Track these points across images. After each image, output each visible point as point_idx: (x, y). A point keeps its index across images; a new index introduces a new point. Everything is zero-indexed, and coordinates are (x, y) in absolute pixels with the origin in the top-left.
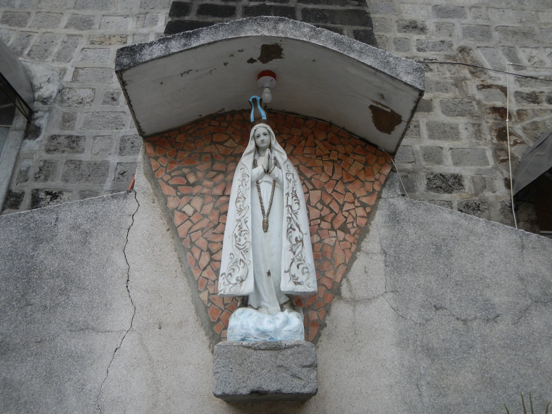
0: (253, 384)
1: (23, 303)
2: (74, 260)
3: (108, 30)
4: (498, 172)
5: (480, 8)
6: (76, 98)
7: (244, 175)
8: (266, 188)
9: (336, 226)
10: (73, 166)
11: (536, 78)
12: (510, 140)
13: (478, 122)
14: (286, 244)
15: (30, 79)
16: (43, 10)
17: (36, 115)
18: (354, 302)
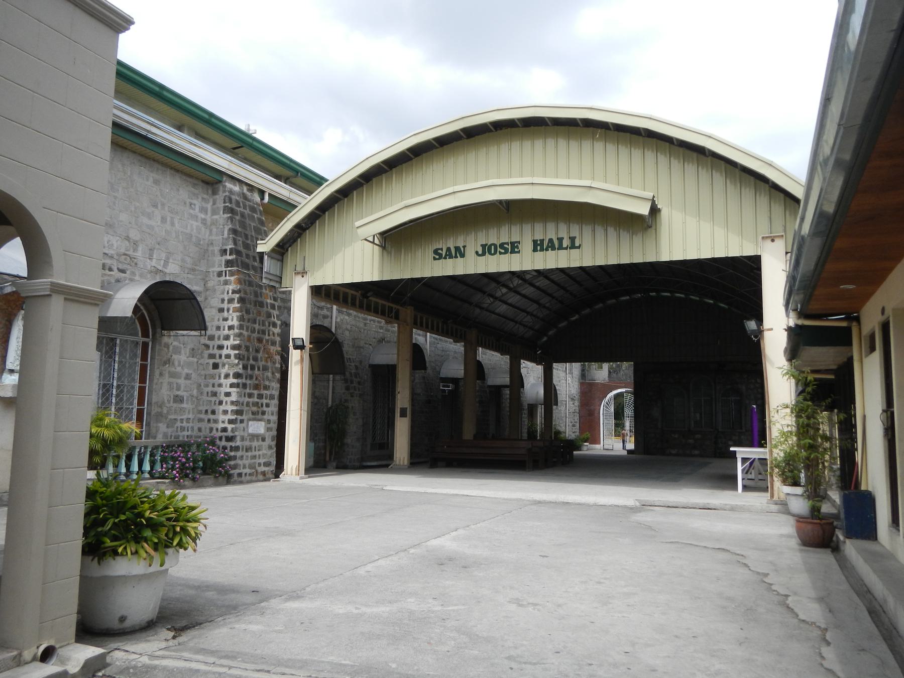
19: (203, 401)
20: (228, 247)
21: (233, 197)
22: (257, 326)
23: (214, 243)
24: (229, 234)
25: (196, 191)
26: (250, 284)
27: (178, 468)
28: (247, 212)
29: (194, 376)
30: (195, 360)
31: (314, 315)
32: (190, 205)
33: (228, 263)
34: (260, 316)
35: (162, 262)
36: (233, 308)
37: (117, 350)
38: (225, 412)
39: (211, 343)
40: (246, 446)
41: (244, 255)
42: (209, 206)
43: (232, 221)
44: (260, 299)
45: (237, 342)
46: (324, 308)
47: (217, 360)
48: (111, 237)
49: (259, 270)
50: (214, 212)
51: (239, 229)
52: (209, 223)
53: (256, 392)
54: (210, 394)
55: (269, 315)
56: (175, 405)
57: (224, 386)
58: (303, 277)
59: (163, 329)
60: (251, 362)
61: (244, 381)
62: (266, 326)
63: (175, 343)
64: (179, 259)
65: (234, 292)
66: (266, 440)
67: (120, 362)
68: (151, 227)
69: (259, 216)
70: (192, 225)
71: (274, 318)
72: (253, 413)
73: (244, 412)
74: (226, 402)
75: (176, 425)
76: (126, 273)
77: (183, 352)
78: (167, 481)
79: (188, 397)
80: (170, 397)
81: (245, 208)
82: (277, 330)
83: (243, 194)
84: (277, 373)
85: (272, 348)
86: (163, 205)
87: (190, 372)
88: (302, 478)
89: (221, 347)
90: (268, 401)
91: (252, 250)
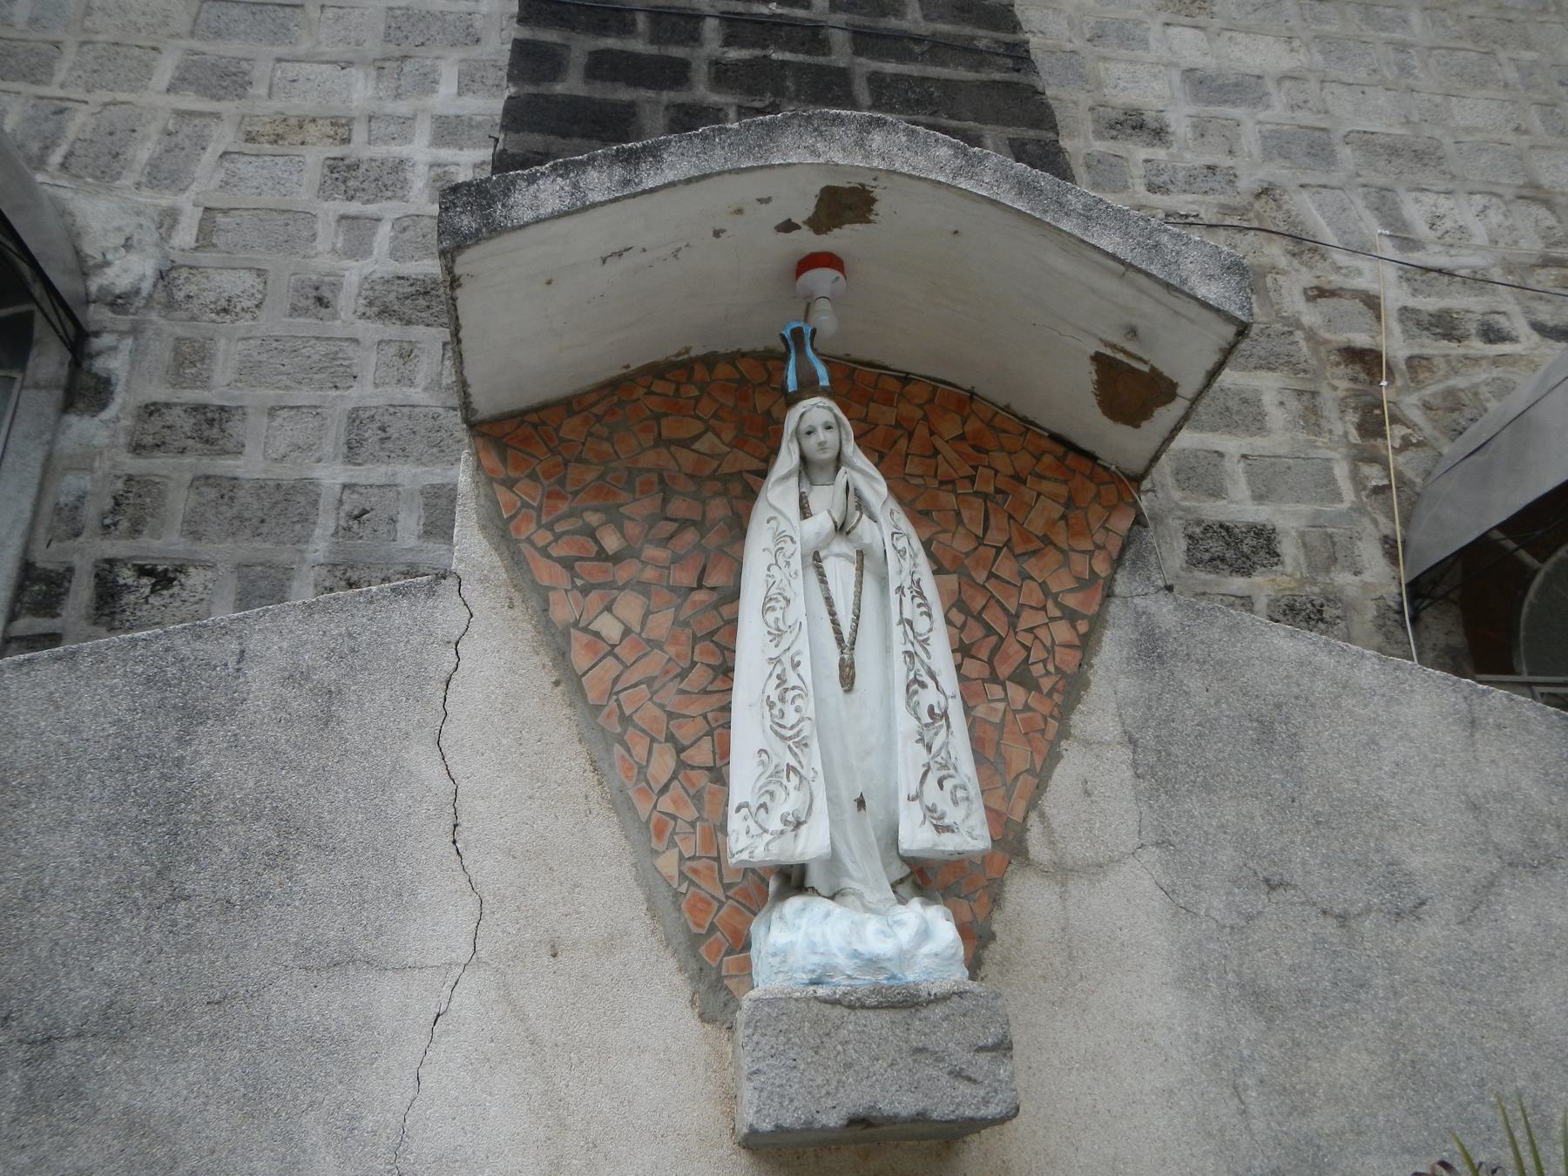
0: (854, 1098)
1: (163, 893)
2: (298, 769)
3: (296, 101)
4: (1366, 521)
5: (1306, 80)
6: (212, 297)
7: (780, 537)
8: (840, 572)
9: (1004, 671)
10: (212, 494)
11: (1451, 274)
12: (1395, 434)
13: (1310, 387)
14: (905, 724)
15: (73, 236)
16: (101, 38)
17: (97, 343)
18: (1061, 872)
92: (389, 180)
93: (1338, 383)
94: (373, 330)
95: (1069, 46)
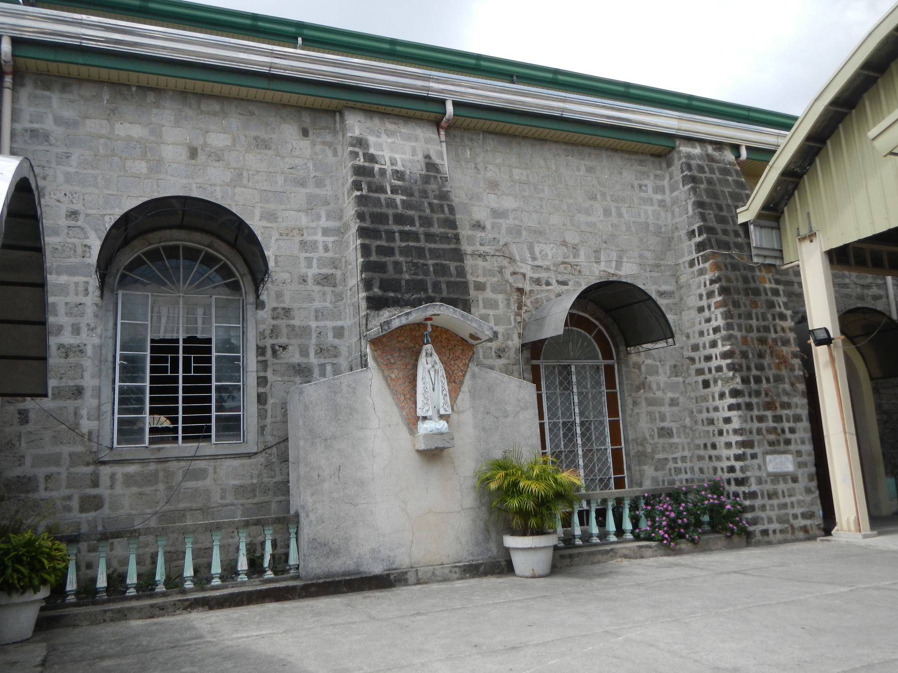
6: (280, 279)
8: (432, 373)
10: (290, 329)
12: (524, 308)
14: (441, 397)
19: (700, 433)
20: (695, 227)
21: (693, 162)
22: (754, 323)
23: (678, 226)
24: (694, 210)
25: (644, 169)
26: (735, 267)
27: (665, 526)
28: (717, 176)
29: (681, 400)
30: (681, 379)
31: (838, 288)
32: (640, 187)
33: (700, 247)
34: (756, 307)
35: (614, 264)
36: (715, 303)
37: (574, 379)
38: (728, 445)
39: (695, 355)
40: (767, 491)
41: (720, 232)
42: (666, 183)
43: (695, 192)
44: (752, 285)
45: (728, 348)
46: (871, 286)
47: (707, 376)
48: (544, 246)
49: (746, 248)
50: (673, 189)
51: (708, 200)
52: (669, 203)
53: (769, 414)
54: (705, 422)
55: (771, 305)
56: (662, 441)
57: (721, 409)
58: (811, 241)
59: (628, 345)
60: (754, 372)
61: (747, 399)
62: (768, 320)
63: (649, 362)
64: (637, 256)
65: (712, 282)
66: (800, 479)
67: (579, 394)
68: (593, 225)
69: (735, 178)
70: (646, 212)
71: (780, 307)
72: (771, 444)
73: (756, 444)
74: (728, 432)
75: (668, 466)
76: (568, 285)
77: (660, 370)
78: (653, 544)
79: (678, 429)
80: (653, 430)
81: (712, 171)
82: (789, 323)
83: (708, 155)
84: (800, 383)
85: (785, 349)
86: (603, 195)
87: (676, 396)
88: (866, 536)
89: (708, 358)
90: (792, 424)
91: (731, 223)
92: (314, 246)
93: (515, 296)
94: (317, 288)
95: (465, 202)
